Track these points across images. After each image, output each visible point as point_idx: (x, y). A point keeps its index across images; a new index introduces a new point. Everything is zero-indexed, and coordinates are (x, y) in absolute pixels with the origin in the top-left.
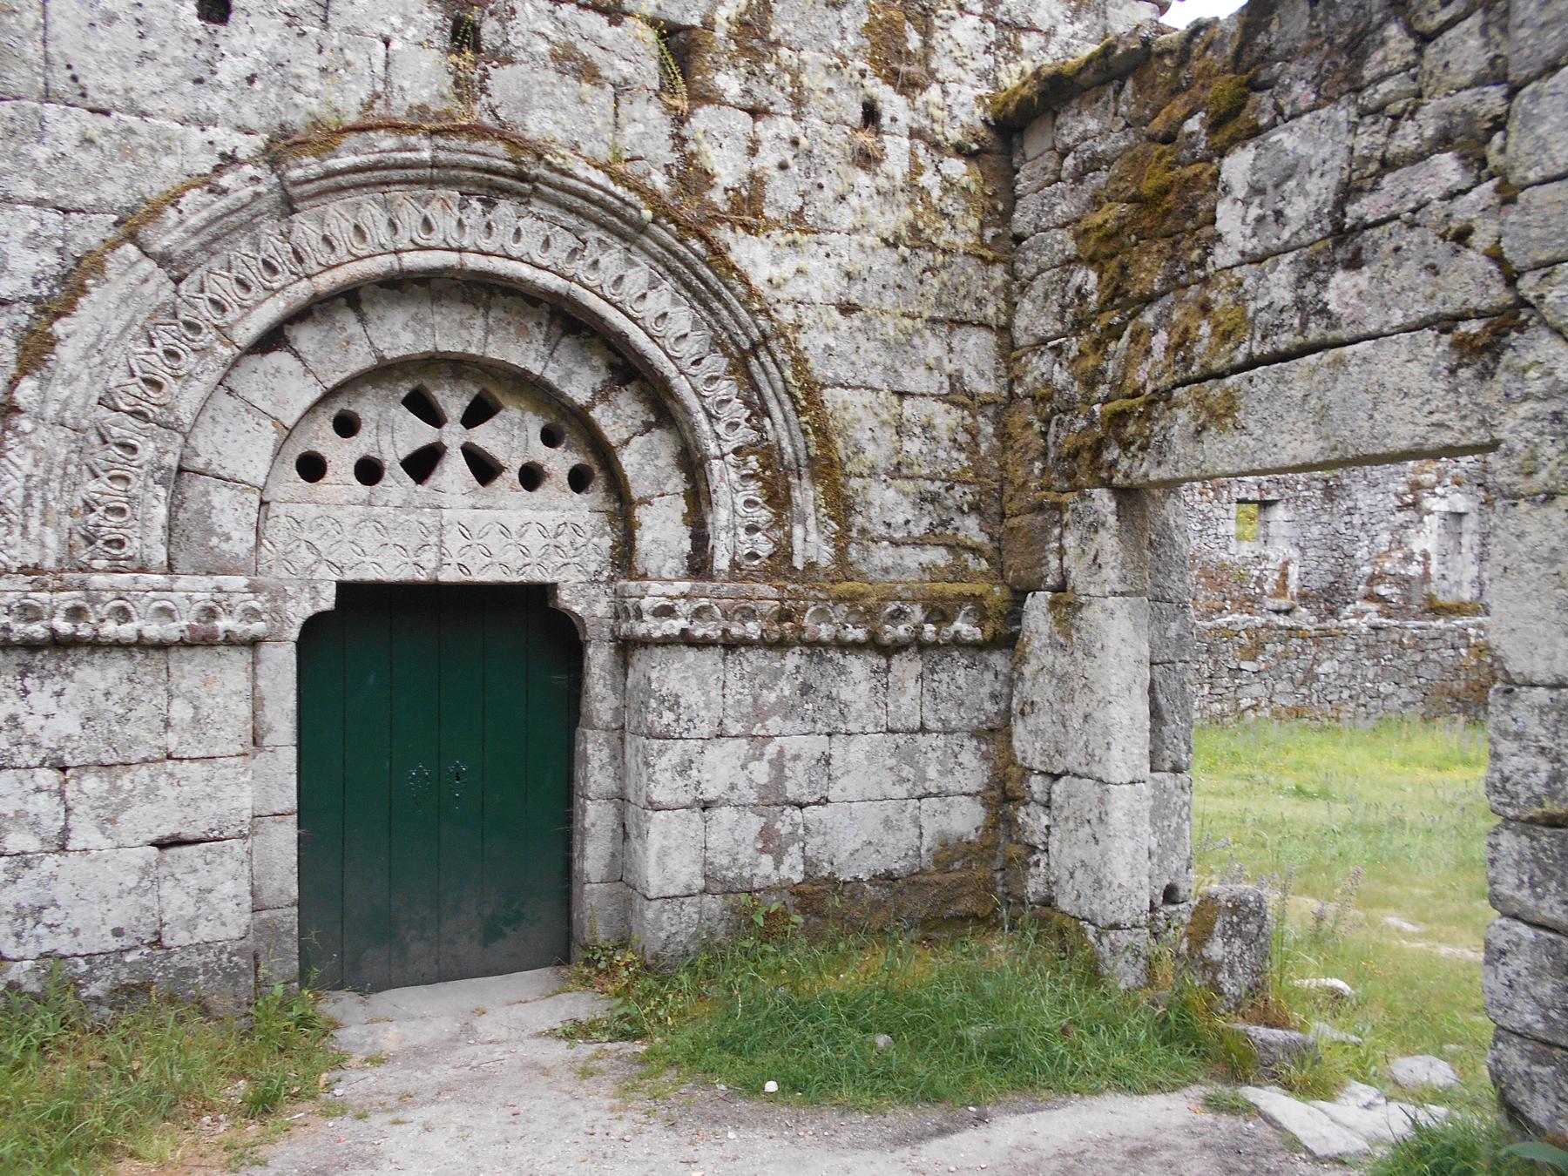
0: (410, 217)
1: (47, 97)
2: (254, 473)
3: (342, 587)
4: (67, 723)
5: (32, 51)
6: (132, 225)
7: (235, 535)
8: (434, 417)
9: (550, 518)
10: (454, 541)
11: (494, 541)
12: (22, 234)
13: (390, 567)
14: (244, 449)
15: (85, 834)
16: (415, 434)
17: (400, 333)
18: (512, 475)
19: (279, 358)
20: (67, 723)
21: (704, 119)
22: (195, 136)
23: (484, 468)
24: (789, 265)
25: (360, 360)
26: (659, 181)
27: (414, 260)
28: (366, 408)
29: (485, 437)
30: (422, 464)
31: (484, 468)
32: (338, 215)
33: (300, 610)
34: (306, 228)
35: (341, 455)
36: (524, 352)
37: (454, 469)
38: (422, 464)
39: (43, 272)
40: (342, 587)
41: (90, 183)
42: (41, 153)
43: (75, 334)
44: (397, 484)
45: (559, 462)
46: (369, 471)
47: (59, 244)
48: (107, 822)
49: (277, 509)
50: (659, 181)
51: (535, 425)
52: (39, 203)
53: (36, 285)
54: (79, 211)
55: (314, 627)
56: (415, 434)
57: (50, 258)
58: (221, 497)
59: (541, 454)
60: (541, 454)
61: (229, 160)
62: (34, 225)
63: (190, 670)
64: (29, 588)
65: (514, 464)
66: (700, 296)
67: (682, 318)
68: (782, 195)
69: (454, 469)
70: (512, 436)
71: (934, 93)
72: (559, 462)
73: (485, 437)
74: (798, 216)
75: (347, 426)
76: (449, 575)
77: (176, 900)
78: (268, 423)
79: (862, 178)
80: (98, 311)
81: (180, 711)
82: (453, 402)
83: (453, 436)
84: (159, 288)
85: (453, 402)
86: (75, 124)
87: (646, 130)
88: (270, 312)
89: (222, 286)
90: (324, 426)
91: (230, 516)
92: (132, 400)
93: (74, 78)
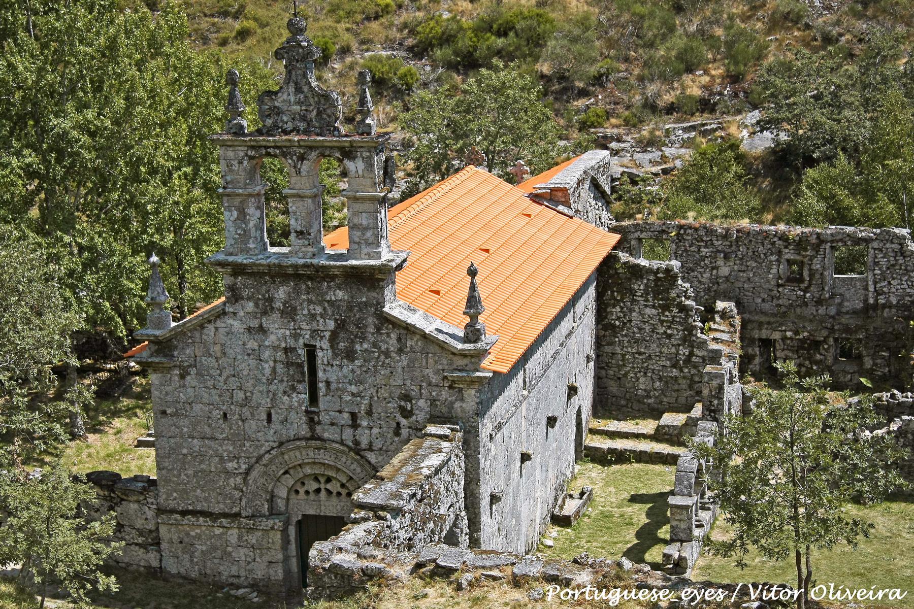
0: (304, 453)
1: (245, 440)
3: (304, 515)
4: (254, 541)
6: (259, 458)
8: (319, 482)
9: (342, 504)
10: (323, 508)
11: (331, 508)
13: (311, 512)
14: (282, 492)
15: (258, 559)
16: (315, 486)
17: (308, 470)
18: (334, 494)
19: (288, 476)
20: (254, 541)
21: (359, 431)
22: (267, 444)
23: (329, 492)
24: (380, 459)
25: (301, 475)
26: (351, 444)
27: (306, 461)
28: (306, 482)
29: (329, 486)
30: (318, 491)
31: (329, 492)
32: (291, 453)
33: (294, 520)
34: (286, 457)
35: (302, 491)
36: (331, 473)
37: (323, 493)
38: (318, 491)
40: (304, 515)
43: (251, 479)
44: (312, 496)
45: (344, 492)
46: (307, 493)
48: (260, 558)
49: (291, 501)
50: (351, 444)
51: (339, 485)
55: (299, 522)
56: (315, 486)
58: (279, 500)
59: (340, 490)
60: (340, 490)
61: (273, 448)
63: (271, 534)
65: (335, 492)
66: (362, 466)
67: (359, 470)
68: (378, 444)
69: (323, 493)
70: (334, 487)
71: (414, 417)
72: (344, 492)
73: (329, 486)
74: (381, 449)
75: (303, 484)
76: (322, 514)
77: (271, 572)
79: (396, 439)
80: (254, 474)
81: (270, 541)
82: (322, 480)
83: (322, 486)
84: (263, 469)
85: (322, 480)
87: (348, 434)
88: (282, 472)
89: (274, 467)
90: (299, 484)
91: (281, 504)
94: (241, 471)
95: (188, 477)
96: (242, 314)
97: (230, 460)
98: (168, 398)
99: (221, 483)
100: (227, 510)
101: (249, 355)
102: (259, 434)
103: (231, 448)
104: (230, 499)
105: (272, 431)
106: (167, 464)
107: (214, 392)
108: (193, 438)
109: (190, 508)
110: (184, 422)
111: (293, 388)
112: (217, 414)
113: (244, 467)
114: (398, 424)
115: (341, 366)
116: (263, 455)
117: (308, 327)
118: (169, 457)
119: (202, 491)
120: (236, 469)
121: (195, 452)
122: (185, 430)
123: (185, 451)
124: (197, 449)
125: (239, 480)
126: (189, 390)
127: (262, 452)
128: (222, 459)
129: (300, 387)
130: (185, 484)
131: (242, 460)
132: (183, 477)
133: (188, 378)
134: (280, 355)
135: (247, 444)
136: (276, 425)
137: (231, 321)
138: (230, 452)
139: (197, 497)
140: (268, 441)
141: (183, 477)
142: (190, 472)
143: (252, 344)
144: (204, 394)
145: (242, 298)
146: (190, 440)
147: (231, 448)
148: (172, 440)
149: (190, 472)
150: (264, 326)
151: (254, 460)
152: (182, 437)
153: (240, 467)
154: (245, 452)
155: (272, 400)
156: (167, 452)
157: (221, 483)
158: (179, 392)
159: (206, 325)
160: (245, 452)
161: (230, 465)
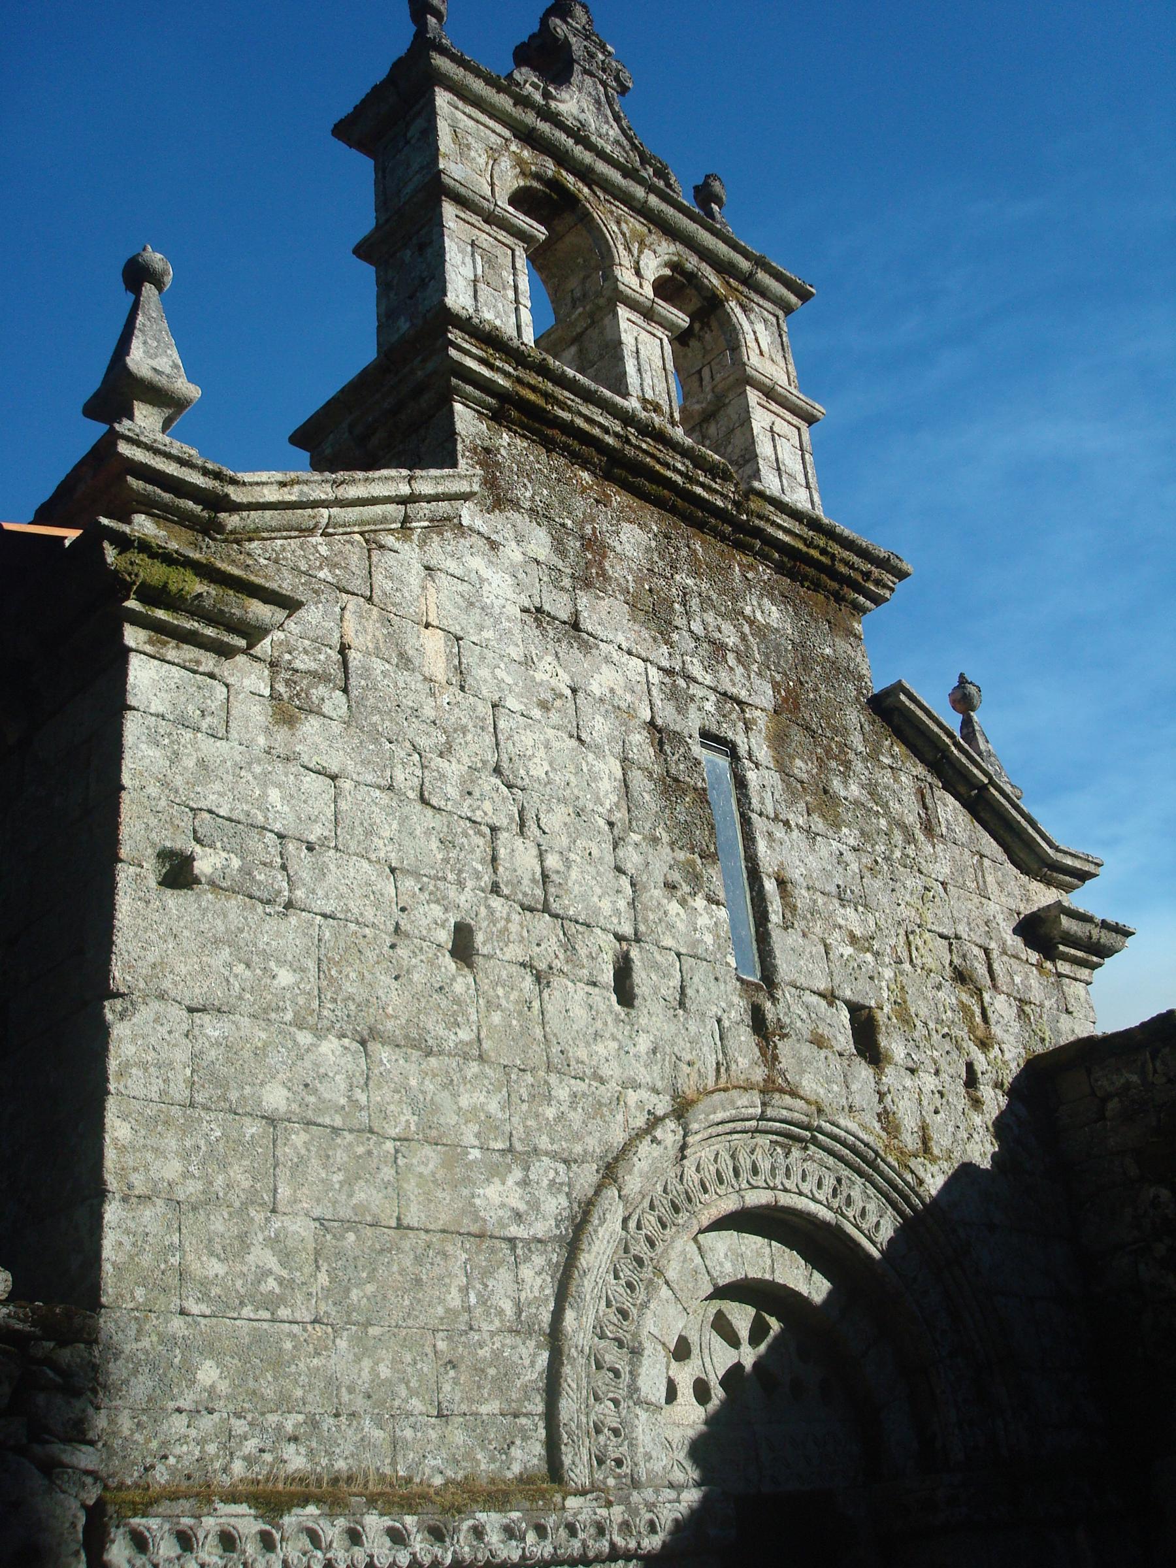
1: (549, 1068)
2: (658, 1394)
5: (538, 1032)
7: (654, 1454)
12: (545, 1182)
39: (560, 1214)
41: (577, 1137)
42: (550, 1113)
47: (567, 1189)
52: (554, 1156)
53: (557, 1226)
54: (576, 1161)
57: (564, 1202)
62: (552, 1174)
64: (595, 1504)
78: (660, 1347)
86: (567, 1089)
92: (611, 1327)
93: (562, 1052)
94: (541, 1228)
95: (286, 1257)
96: (513, 553)
97: (496, 1172)
98: (212, 796)
99: (454, 1299)
100: (485, 1465)
101: (544, 706)
102: (600, 1048)
103: (493, 1107)
104: (501, 1385)
105: (644, 1044)
106: (172, 1169)
107: (424, 819)
108: (319, 1034)
109: (296, 1460)
110: (286, 935)
111: (695, 879)
112: (433, 923)
113: (555, 1205)
114: (970, 1066)
115: (811, 835)
116: (627, 1149)
117: (708, 680)
118: (186, 1129)
119: (364, 1348)
120: (518, 1216)
121: (325, 1106)
122: (285, 977)
123: (275, 1098)
124: (335, 1092)
125: (535, 1278)
126: (313, 783)
127: (619, 1137)
128: (454, 1153)
129: (714, 875)
130: (270, 1303)
131: (544, 1170)
132: (262, 1256)
133: (311, 726)
134: (640, 743)
135: (562, 1093)
136: (653, 1015)
137: (477, 563)
138: (490, 1126)
139: (332, 1383)
140: (636, 1086)
141: (262, 1256)
142: (300, 1228)
143: (551, 673)
144: (379, 817)
145: (516, 505)
146: (304, 1038)
147: (493, 1107)
148: (212, 1028)
149: (300, 1228)
150: (587, 624)
151: (587, 1176)
152: (261, 1016)
153: (535, 1205)
154: (548, 1127)
155: (632, 904)
156: (179, 1091)
157: (454, 1299)
158: (264, 780)
159: (389, 540)
160: (548, 1127)
161: (497, 1196)
